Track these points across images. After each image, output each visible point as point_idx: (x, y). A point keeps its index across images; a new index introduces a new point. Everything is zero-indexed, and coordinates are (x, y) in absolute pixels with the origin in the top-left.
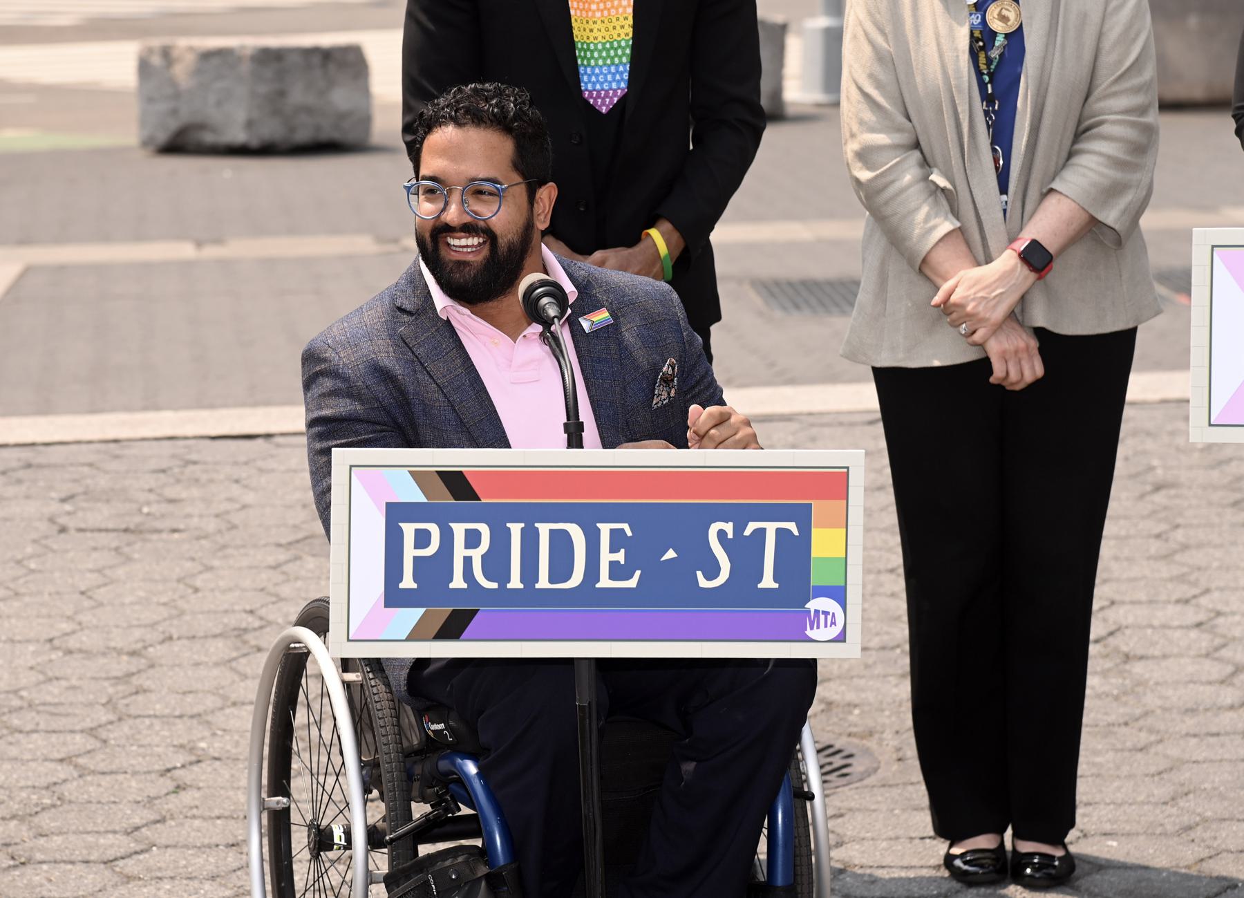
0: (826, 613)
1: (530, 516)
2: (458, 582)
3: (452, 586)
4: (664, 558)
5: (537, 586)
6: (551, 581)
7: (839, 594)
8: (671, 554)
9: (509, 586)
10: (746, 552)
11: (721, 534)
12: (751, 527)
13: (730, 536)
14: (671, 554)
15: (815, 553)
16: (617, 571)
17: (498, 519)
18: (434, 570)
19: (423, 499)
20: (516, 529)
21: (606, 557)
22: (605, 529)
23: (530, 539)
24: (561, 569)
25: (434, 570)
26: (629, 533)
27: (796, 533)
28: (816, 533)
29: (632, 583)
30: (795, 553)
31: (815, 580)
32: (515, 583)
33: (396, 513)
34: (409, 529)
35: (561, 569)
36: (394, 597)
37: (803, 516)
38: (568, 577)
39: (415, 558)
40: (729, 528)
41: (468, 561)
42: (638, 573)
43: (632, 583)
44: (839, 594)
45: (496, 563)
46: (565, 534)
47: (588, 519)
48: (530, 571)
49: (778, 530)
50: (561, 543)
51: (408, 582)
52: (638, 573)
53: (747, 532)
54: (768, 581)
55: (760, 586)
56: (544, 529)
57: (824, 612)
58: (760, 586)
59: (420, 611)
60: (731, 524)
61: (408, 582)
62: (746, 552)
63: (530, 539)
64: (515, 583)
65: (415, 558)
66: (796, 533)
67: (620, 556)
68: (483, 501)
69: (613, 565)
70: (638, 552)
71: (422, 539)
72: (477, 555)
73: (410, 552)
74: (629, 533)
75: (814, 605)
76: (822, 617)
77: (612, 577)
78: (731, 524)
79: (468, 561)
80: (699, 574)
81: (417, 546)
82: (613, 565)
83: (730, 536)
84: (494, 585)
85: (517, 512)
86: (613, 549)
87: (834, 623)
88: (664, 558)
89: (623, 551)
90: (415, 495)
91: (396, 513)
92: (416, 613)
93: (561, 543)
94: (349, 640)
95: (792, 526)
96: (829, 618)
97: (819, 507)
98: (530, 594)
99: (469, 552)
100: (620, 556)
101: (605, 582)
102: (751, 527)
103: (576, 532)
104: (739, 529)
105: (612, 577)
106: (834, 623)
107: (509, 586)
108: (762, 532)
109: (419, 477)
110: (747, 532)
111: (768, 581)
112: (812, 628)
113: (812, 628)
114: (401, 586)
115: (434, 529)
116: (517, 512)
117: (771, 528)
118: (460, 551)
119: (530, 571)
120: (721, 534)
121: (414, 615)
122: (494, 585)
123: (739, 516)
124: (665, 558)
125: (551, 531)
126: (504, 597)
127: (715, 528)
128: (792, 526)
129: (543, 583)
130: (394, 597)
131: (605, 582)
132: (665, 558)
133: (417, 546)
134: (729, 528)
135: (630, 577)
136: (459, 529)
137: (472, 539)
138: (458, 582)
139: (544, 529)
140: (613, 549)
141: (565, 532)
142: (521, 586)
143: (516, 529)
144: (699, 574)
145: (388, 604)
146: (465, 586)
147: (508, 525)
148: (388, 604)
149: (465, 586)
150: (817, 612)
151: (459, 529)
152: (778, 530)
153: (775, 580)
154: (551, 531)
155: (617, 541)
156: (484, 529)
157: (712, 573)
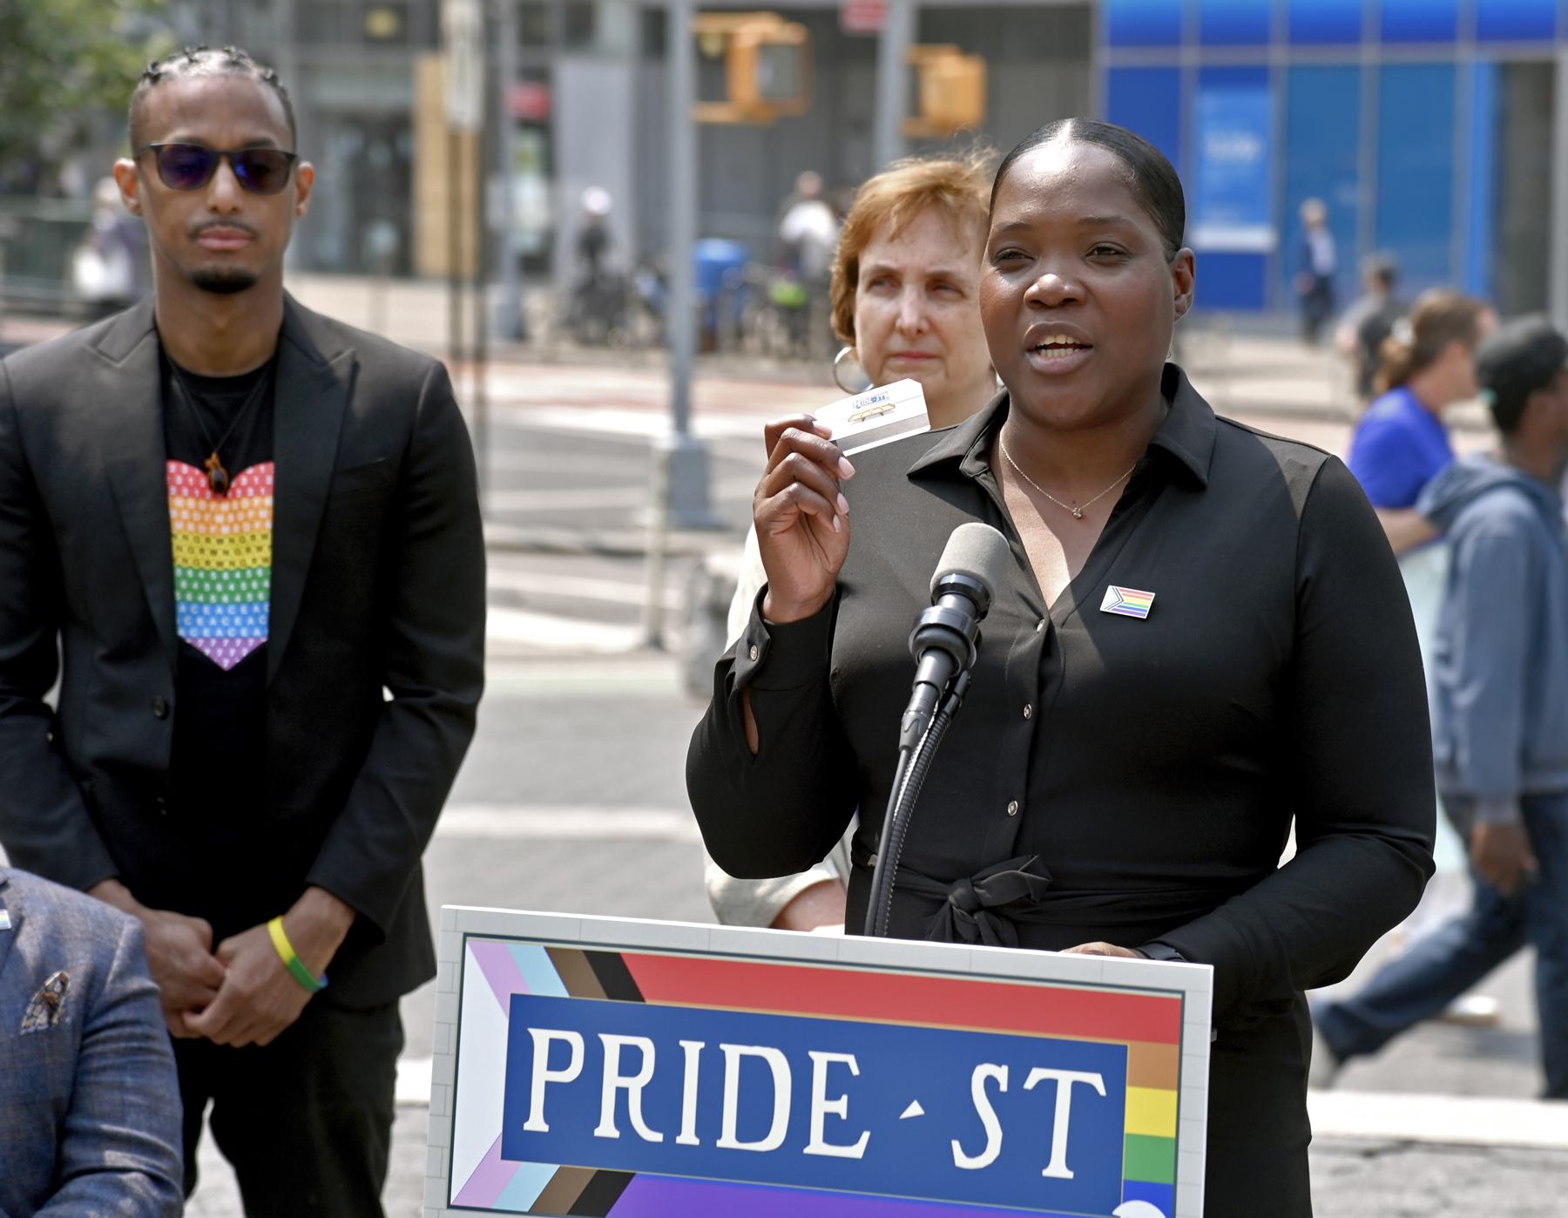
1: (716, 1030)
2: (607, 1128)
4: (904, 1115)
5: (720, 1144)
7: (1163, 1196)
8: (915, 1110)
9: (679, 1140)
10: (1026, 1114)
11: (991, 1083)
12: (1036, 1075)
13: (1004, 1087)
14: (915, 1110)
15: (1132, 1125)
16: (837, 1131)
18: (573, 1105)
20: (692, 1050)
21: (820, 1106)
23: (712, 1067)
24: (755, 1120)
25: (573, 1105)
26: (855, 1071)
27: (1102, 1092)
28: (1132, 1093)
29: (857, 1151)
31: (1129, 1172)
32: (688, 1136)
33: (525, 1012)
34: (541, 1038)
35: (755, 1120)
36: (516, 1145)
37: (1113, 1065)
38: (763, 1133)
39: (548, 1084)
40: (1001, 1074)
41: (622, 1094)
42: (866, 1136)
43: (857, 1151)
45: (662, 1102)
48: (709, 1122)
51: (536, 1122)
52: (866, 1136)
53: (1030, 1084)
54: (1058, 1168)
56: (733, 1053)
59: (550, 1170)
60: (1005, 1069)
61: (536, 1122)
62: (1026, 1114)
63: (712, 1067)
64: (688, 1136)
65: (548, 1084)
67: (841, 1107)
68: (649, 1002)
69: (830, 1118)
70: (868, 1104)
72: (635, 1086)
73: (541, 1075)
74: (855, 1071)
77: (829, 1138)
78: (1005, 1069)
79: (622, 1094)
80: (956, 1145)
82: (830, 1118)
83: (1004, 1087)
84: (657, 1137)
85: (696, 1025)
86: (832, 1095)
88: (904, 1115)
89: (845, 1098)
92: (550, 1170)
93: (756, 1076)
94: (450, 1206)
95: (1096, 1080)
97: (1137, 1053)
99: (625, 1082)
100: (841, 1107)
101: (817, 1146)
102: (1036, 1075)
103: (777, 1061)
104: (1017, 1077)
108: (1049, 1086)
109: (559, 957)
110: (1030, 1084)
111: (1058, 1168)
117: (1065, 1079)
118: (612, 1079)
119: (709, 1122)
120: (991, 1083)
122: (657, 1137)
127: (981, 1072)
128: (1096, 1080)
129: (728, 1139)
131: (817, 1146)
134: (1001, 1074)
135: (853, 1141)
136: (612, 1044)
138: (607, 1128)
139: (733, 1053)
140: (832, 1095)
143: (692, 1050)
144: (956, 1145)
145: (506, 1155)
146: (616, 1134)
148: (506, 1155)
151: (612, 1044)
153: (1069, 1165)
155: (838, 1081)
156: (647, 1046)
157: (975, 1146)
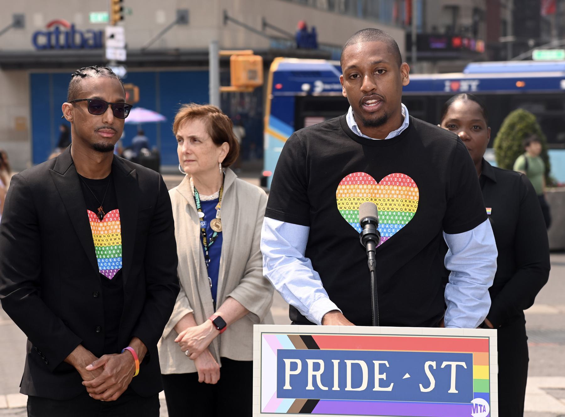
0: (481, 406)
1: (343, 356)
2: (310, 387)
3: (307, 388)
4: (404, 378)
5: (346, 389)
6: (352, 387)
7: (487, 397)
8: (407, 376)
9: (333, 389)
10: (442, 375)
11: (431, 367)
12: (444, 364)
13: (435, 368)
14: (407, 376)
15: (475, 377)
16: (382, 383)
17: (328, 357)
18: (299, 381)
19: (294, 348)
20: (336, 362)
21: (377, 376)
22: (377, 363)
23: (342, 368)
24: (357, 382)
25: (299, 381)
26: (388, 366)
27: (465, 367)
28: (474, 367)
29: (390, 389)
30: (465, 376)
31: (475, 390)
32: (336, 388)
33: (282, 354)
34: (288, 362)
35: (357, 382)
36: (281, 393)
37: (468, 359)
38: (360, 386)
39: (291, 375)
40: (434, 364)
41: (314, 377)
42: (392, 384)
43: (390, 389)
44: (487, 397)
45: (327, 378)
46: (359, 365)
47: (369, 358)
48: (342, 383)
49: (457, 366)
50: (357, 369)
51: (287, 386)
52: (392, 384)
53: (443, 366)
54: (453, 390)
55: (449, 392)
56: (349, 363)
57: (480, 405)
58: (449, 392)
60: (435, 362)
61: (287, 386)
62: (442, 375)
63: (342, 368)
64: (336, 388)
65: (291, 375)
66: (465, 367)
67: (384, 376)
69: (381, 380)
70: (392, 375)
71: (294, 367)
72: (318, 374)
73: (288, 373)
74: (388, 366)
75: (475, 401)
76: (479, 407)
77: (380, 386)
78: (435, 362)
79: (314, 377)
80: (421, 385)
81: (291, 370)
82: (381, 380)
83: (435, 368)
84: (326, 389)
85: (336, 355)
86: (381, 373)
87: (484, 410)
88: (404, 378)
89: (385, 374)
90: (289, 346)
91: (282, 354)
92: (292, 400)
93: (357, 369)
94: (261, 413)
95: (463, 364)
96: (482, 408)
97: (475, 355)
98: (343, 394)
99: (315, 373)
100: (384, 376)
101: (377, 388)
102: (444, 364)
103: (363, 365)
104: (439, 365)
105: (380, 386)
106: (484, 410)
107: (333, 389)
108: (449, 367)
109: (292, 338)
110: (443, 366)
111: (453, 390)
112: (474, 413)
113: (474, 413)
114: (285, 388)
115: (299, 362)
116: (336, 355)
117: (454, 364)
118: (311, 373)
119: (342, 383)
120: (431, 367)
121: (289, 402)
122: (326, 389)
123: (439, 359)
124: (405, 377)
125: (352, 364)
126: (331, 394)
127: (427, 364)
128: (463, 364)
129: (349, 388)
130: (281, 393)
131: (377, 388)
132: (405, 377)
133: (291, 370)
134: (434, 364)
135: (388, 386)
136: (310, 362)
137: (316, 367)
138: (310, 387)
139: (349, 363)
140: (381, 373)
141: (359, 365)
142: (339, 389)
143: (336, 362)
144: (421, 385)
145: (279, 396)
146: (313, 389)
147: (333, 361)
148: (279, 396)
149: (313, 389)
150: (476, 405)
151: (310, 362)
152: (457, 366)
153: (456, 389)
154: (352, 364)
155: (382, 368)
156: (321, 362)
157: (427, 385)
